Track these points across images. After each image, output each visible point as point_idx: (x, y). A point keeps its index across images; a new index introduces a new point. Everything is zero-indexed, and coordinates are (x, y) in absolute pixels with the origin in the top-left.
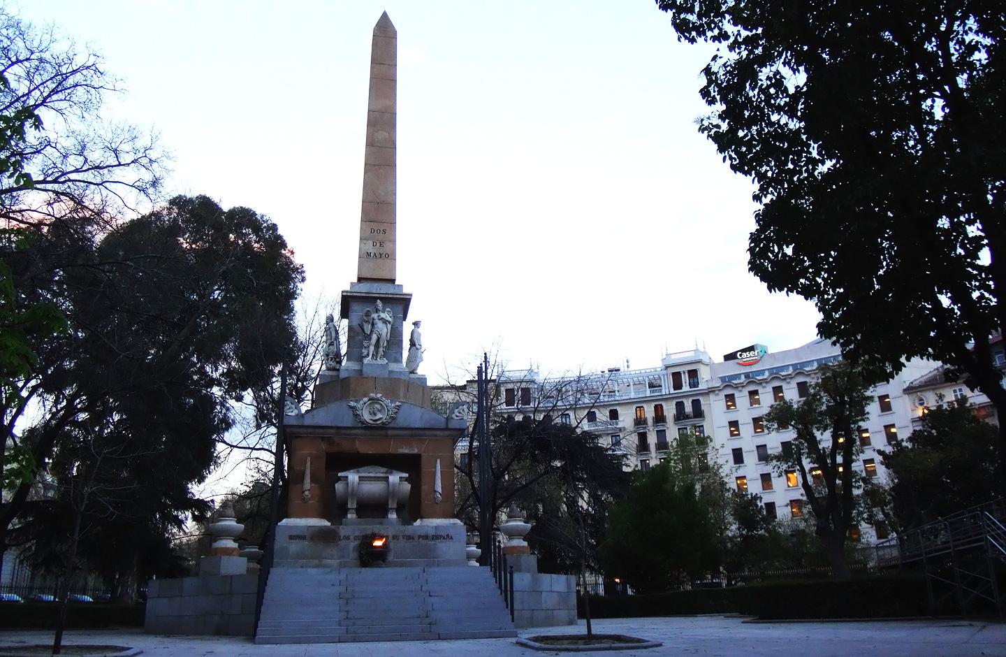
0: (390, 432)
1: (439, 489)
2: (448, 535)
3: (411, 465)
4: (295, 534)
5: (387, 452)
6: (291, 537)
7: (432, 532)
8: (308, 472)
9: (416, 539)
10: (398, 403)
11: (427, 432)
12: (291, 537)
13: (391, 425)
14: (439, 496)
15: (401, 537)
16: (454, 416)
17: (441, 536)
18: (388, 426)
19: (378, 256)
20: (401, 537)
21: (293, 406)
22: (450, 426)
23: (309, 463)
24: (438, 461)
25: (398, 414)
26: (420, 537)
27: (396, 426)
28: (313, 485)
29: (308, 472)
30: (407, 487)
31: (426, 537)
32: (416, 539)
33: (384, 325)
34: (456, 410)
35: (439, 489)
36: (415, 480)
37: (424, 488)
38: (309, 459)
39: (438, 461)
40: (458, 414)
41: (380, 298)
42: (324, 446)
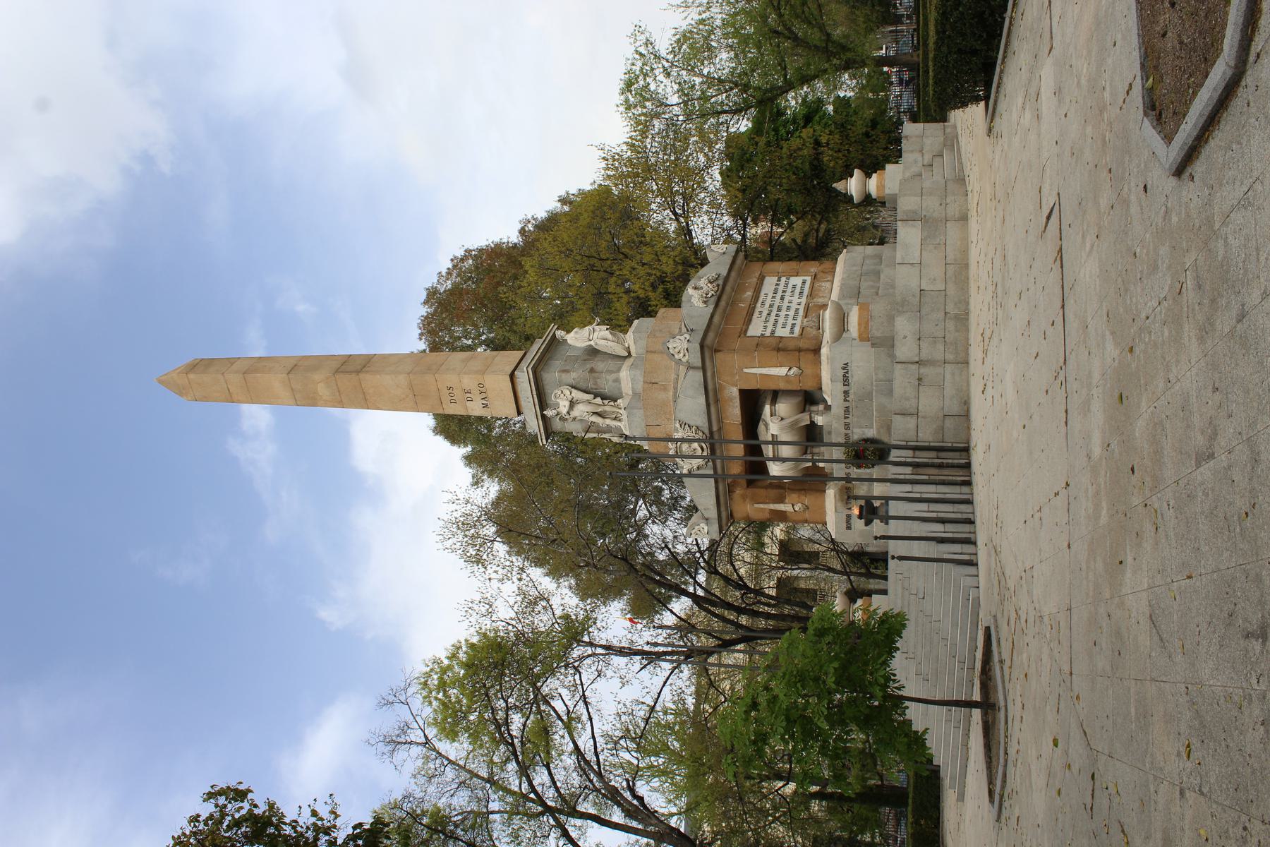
0: (715, 428)
1: (782, 371)
2: (844, 368)
3: (752, 402)
4: (845, 525)
5: (741, 427)
6: (849, 528)
7: (840, 387)
8: (772, 506)
9: (847, 404)
10: (678, 425)
11: (710, 387)
12: (849, 528)
13: (707, 431)
14: (792, 372)
15: (847, 421)
16: (684, 360)
17: (844, 376)
18: (708, 435)
19: (484, 395)
20: (847, 421)
21: (697, 527)
22: (700, 364)
23: (762, 506)
24: (745, 370)
25: (691, 424)
26: (845, 400)
27: (707, 424)
28: (787, 501)
29: (772, 506)
30: (783, 407)
31: (846, 393)
32: (847, 404)
33: (575, 409)
34: (676, 356)
35: (782, 371)
36: (775, 395)
37: (782, 386)
38: (756, 506)
39: (745, 370)
40: (682, 355)
41: (542, 409)
42: (738, 492)
